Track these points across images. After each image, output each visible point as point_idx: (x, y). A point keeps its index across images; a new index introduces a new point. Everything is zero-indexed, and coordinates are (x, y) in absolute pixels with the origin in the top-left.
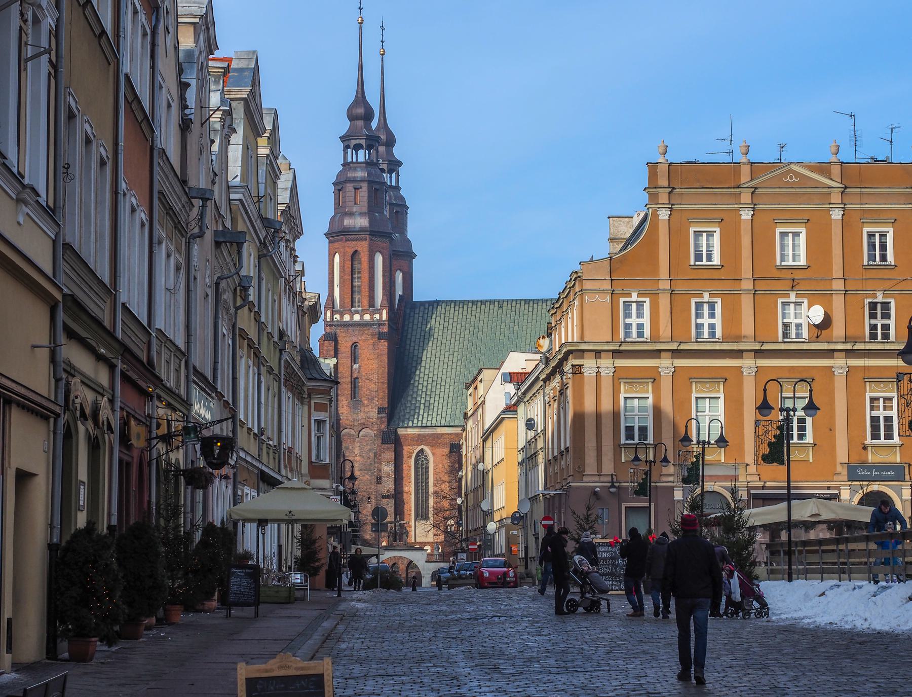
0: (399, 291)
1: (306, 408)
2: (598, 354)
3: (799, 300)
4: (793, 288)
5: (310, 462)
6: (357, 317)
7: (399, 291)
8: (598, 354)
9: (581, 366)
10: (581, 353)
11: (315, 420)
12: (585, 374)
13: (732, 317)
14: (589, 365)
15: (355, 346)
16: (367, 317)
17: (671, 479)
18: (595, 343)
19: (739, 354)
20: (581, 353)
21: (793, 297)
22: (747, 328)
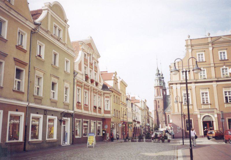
0: (165, 94)
1: (102, 98)
2: (176, 84)
3: (226, 67)
4: (224, 65)
5: (104, 110)
6: (159, 97)
7: (165, 94)
8: (176, 84)
9: (172, 87)
10: (172, 84)
11: (106, 100)
12: (174, 89)
13: (209, 73)
14: (174, 86)
15: (159, 101)
16: (160, 97)
17: (197, 113)
18: (175, 81)
19: (212, 82)
20: (172, 84)
21: (224, 67)
22: (213, 75)
